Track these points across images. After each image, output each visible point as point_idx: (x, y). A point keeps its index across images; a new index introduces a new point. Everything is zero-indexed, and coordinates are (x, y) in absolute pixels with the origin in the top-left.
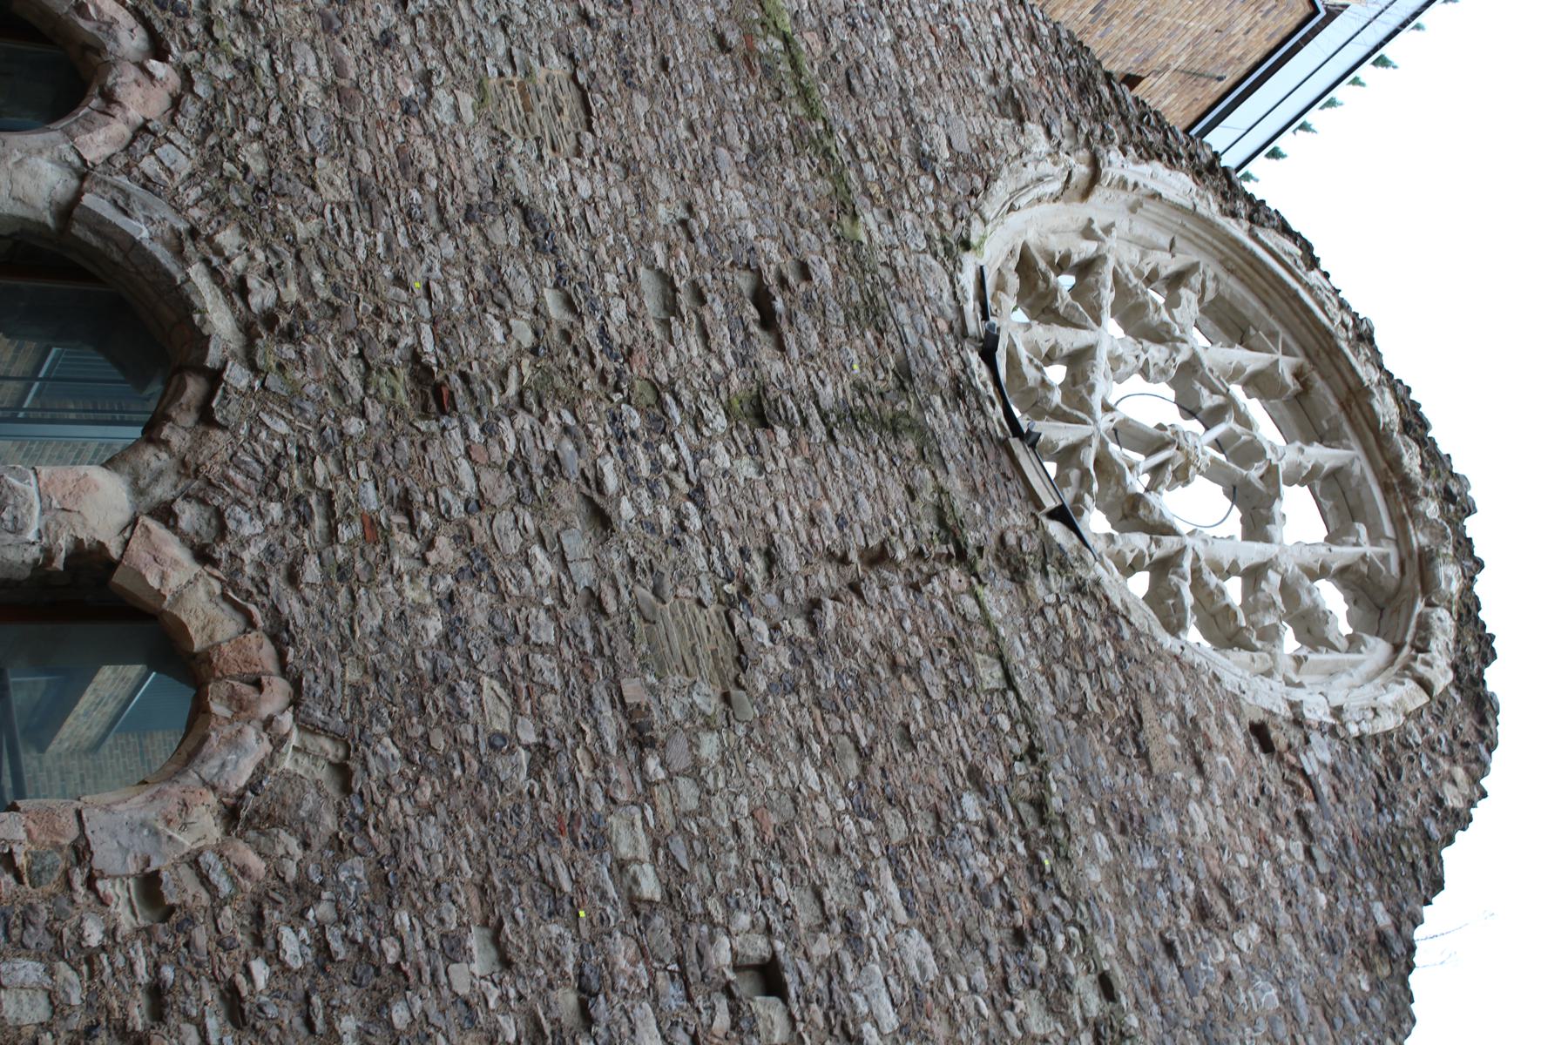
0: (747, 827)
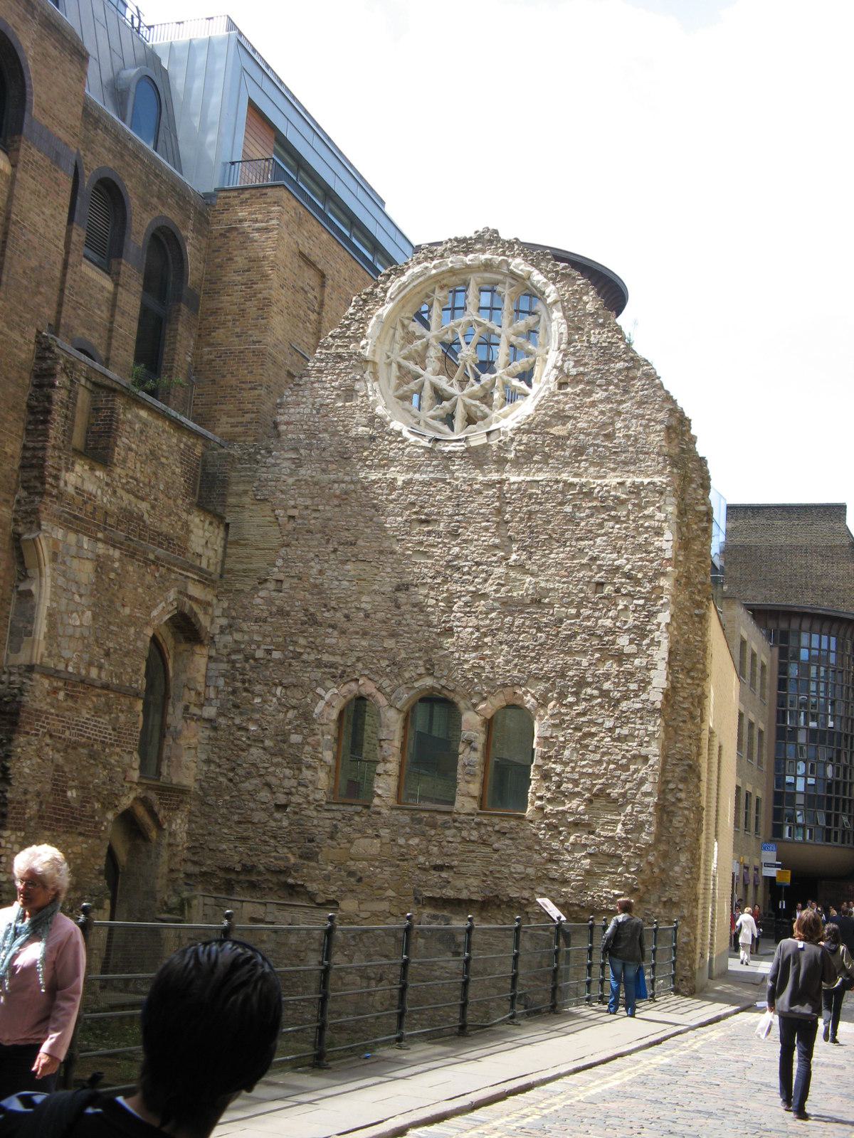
0: (565, 579)
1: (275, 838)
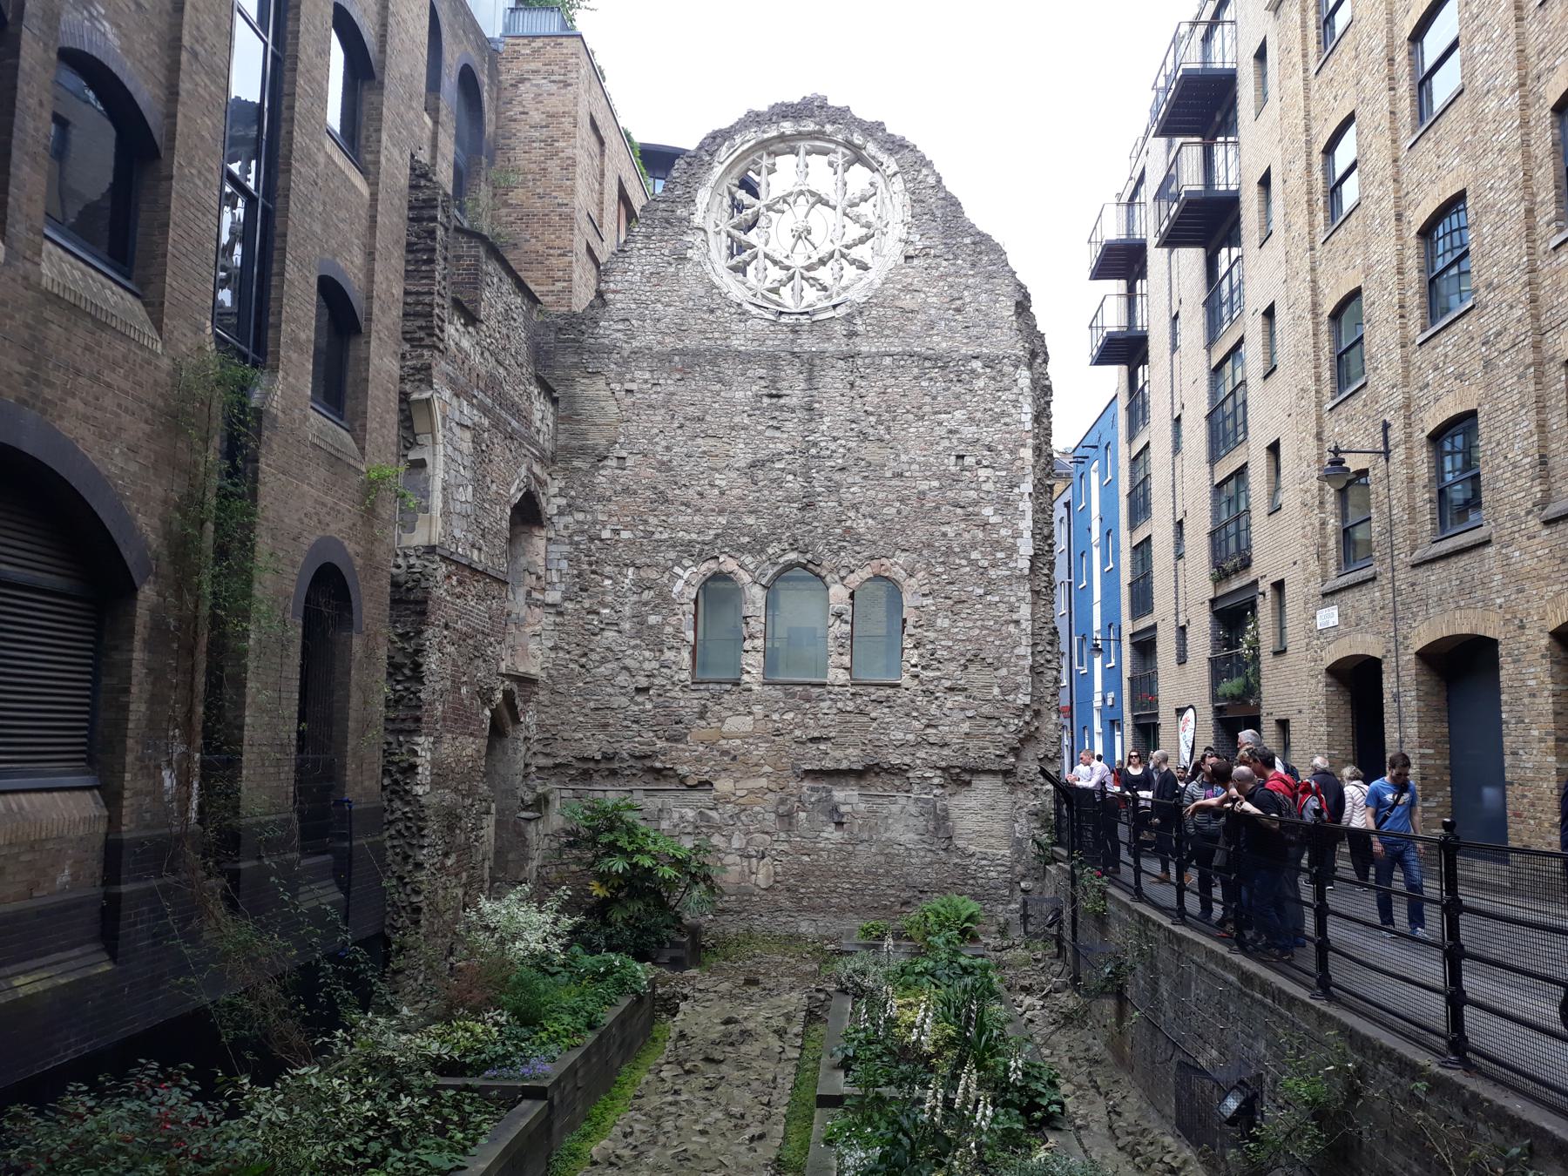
1: (634, 722)
